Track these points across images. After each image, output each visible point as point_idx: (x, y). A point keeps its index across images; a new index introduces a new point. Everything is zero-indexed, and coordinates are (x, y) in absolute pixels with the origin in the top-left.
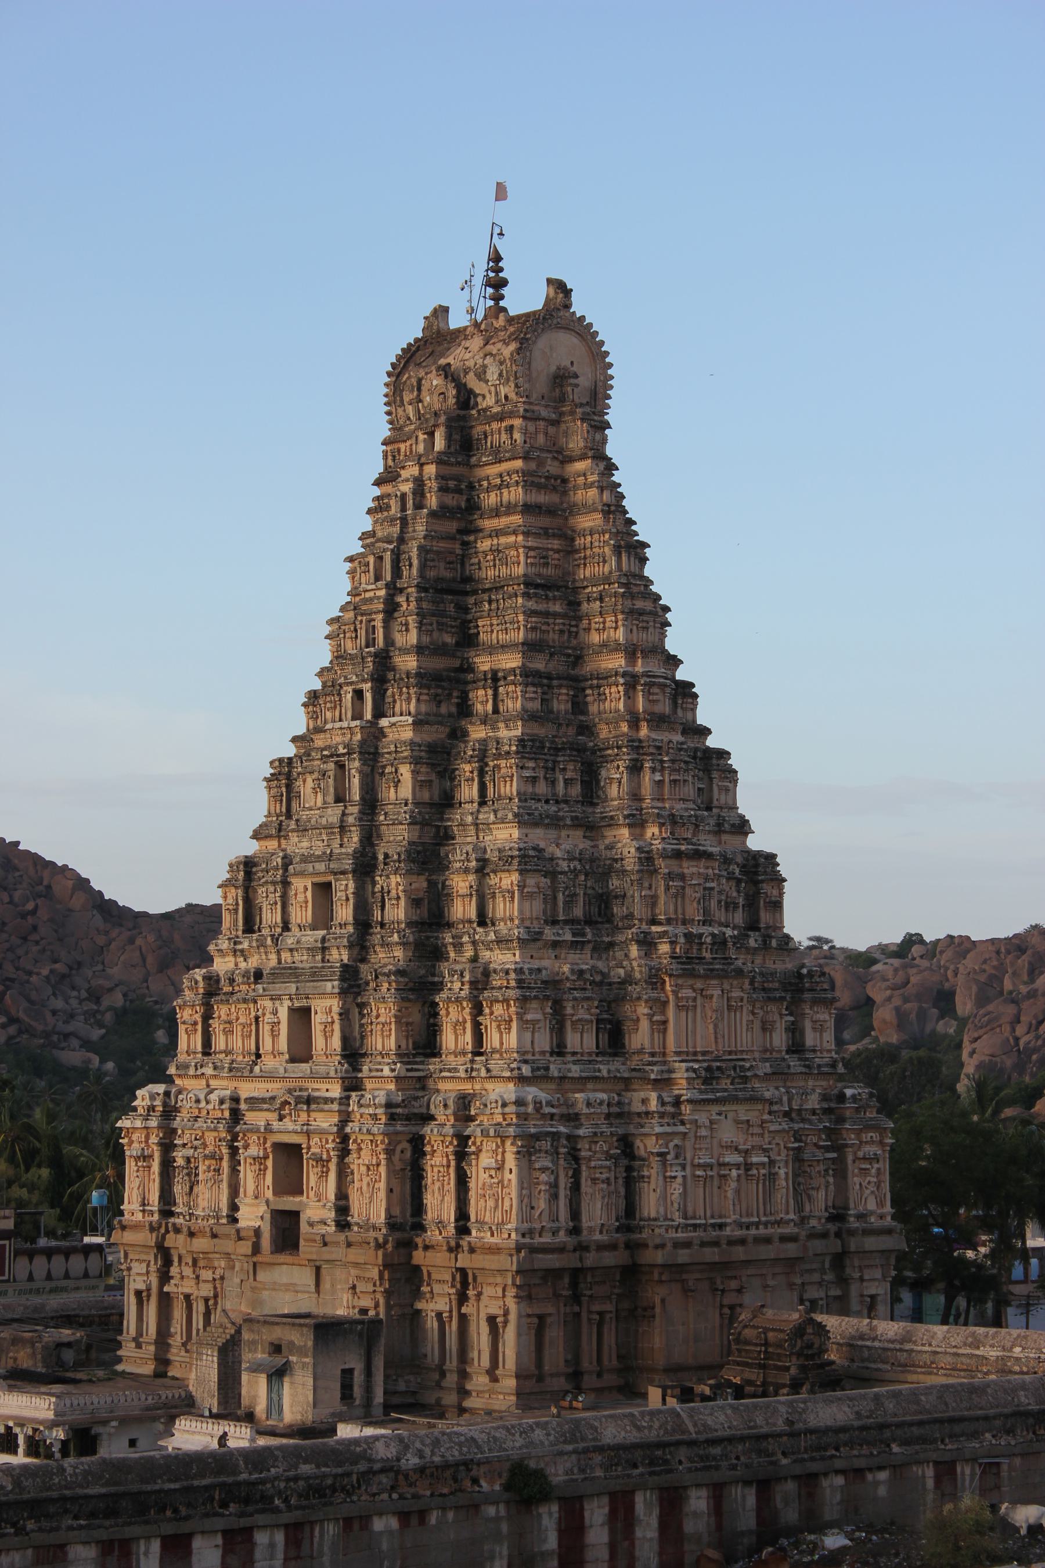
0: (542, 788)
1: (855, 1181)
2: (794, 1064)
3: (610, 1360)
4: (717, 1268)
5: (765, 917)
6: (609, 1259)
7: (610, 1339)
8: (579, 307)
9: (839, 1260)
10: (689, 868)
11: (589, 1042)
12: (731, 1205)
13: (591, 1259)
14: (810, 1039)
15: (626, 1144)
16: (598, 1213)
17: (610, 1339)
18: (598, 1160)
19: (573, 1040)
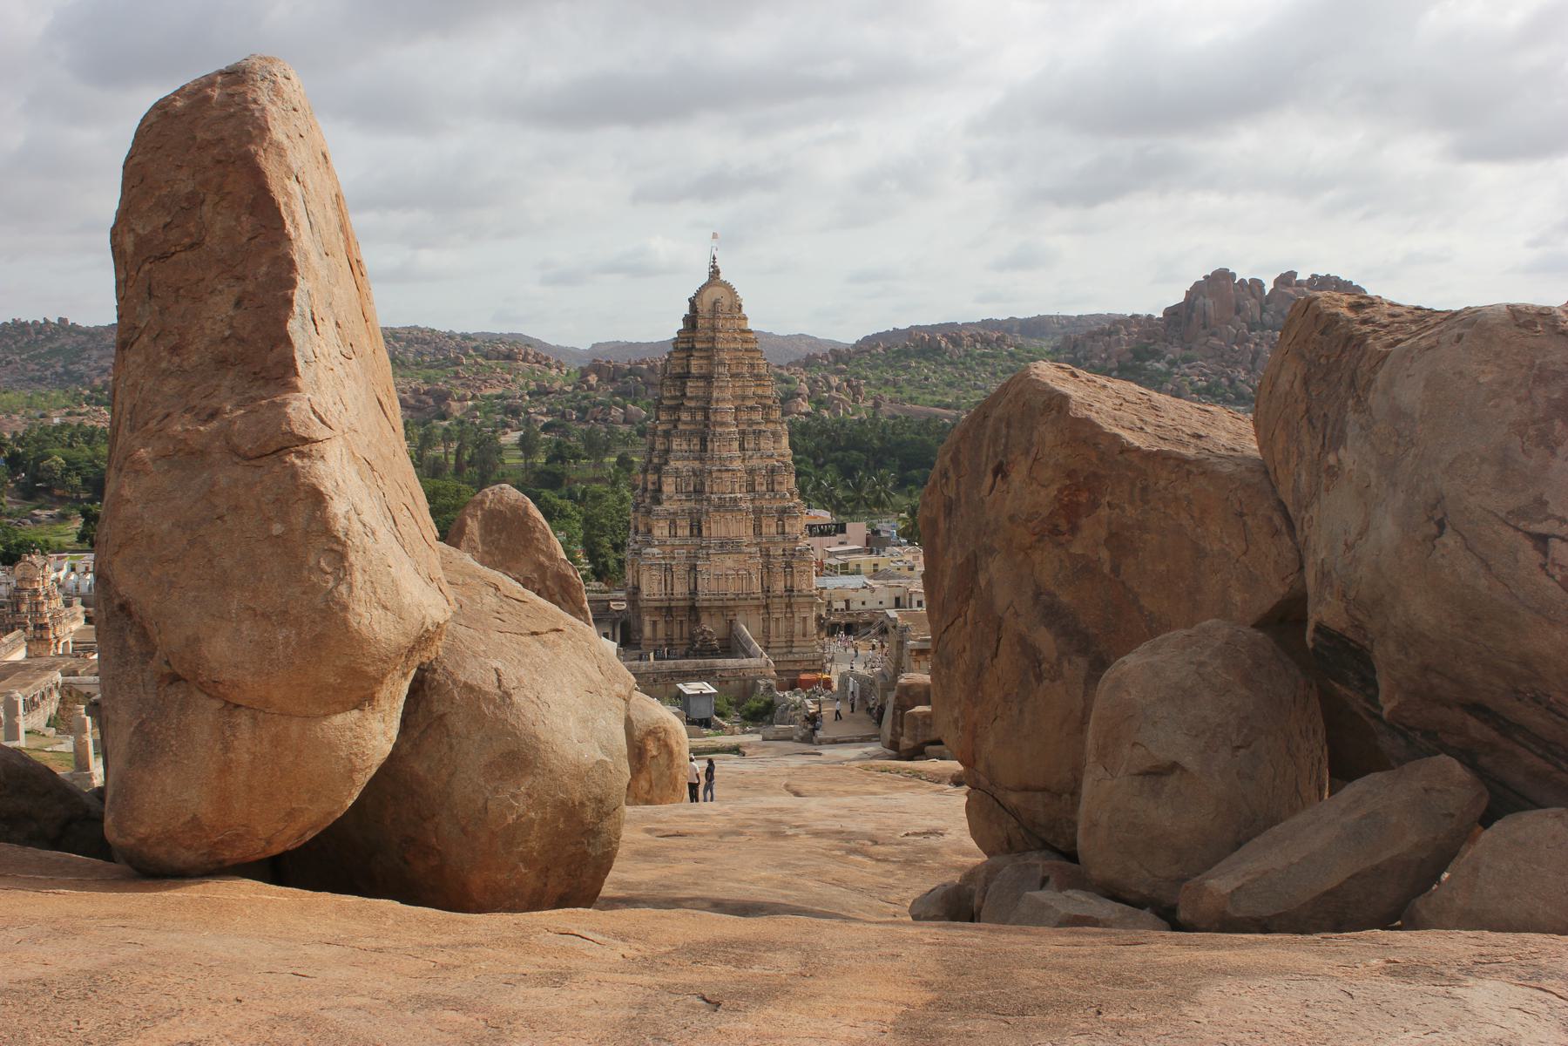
0: (685, 447)
1: (797, 578)
2: (779, 538)
3: (685, 634)
4: (725, 609)
5: (777, 487)
6: (682, 604)
7: (685, 629)
8: (723, 277)
9: (789, 605)
10: (725, 475)
11: (687, 532)
12: (732, 588)
13: (673, 604)
14: (787, 529)
15: (693, 567)
16: (680, 589)
17: (685, 629)
18: (680, 571)
19: (679, 532)
